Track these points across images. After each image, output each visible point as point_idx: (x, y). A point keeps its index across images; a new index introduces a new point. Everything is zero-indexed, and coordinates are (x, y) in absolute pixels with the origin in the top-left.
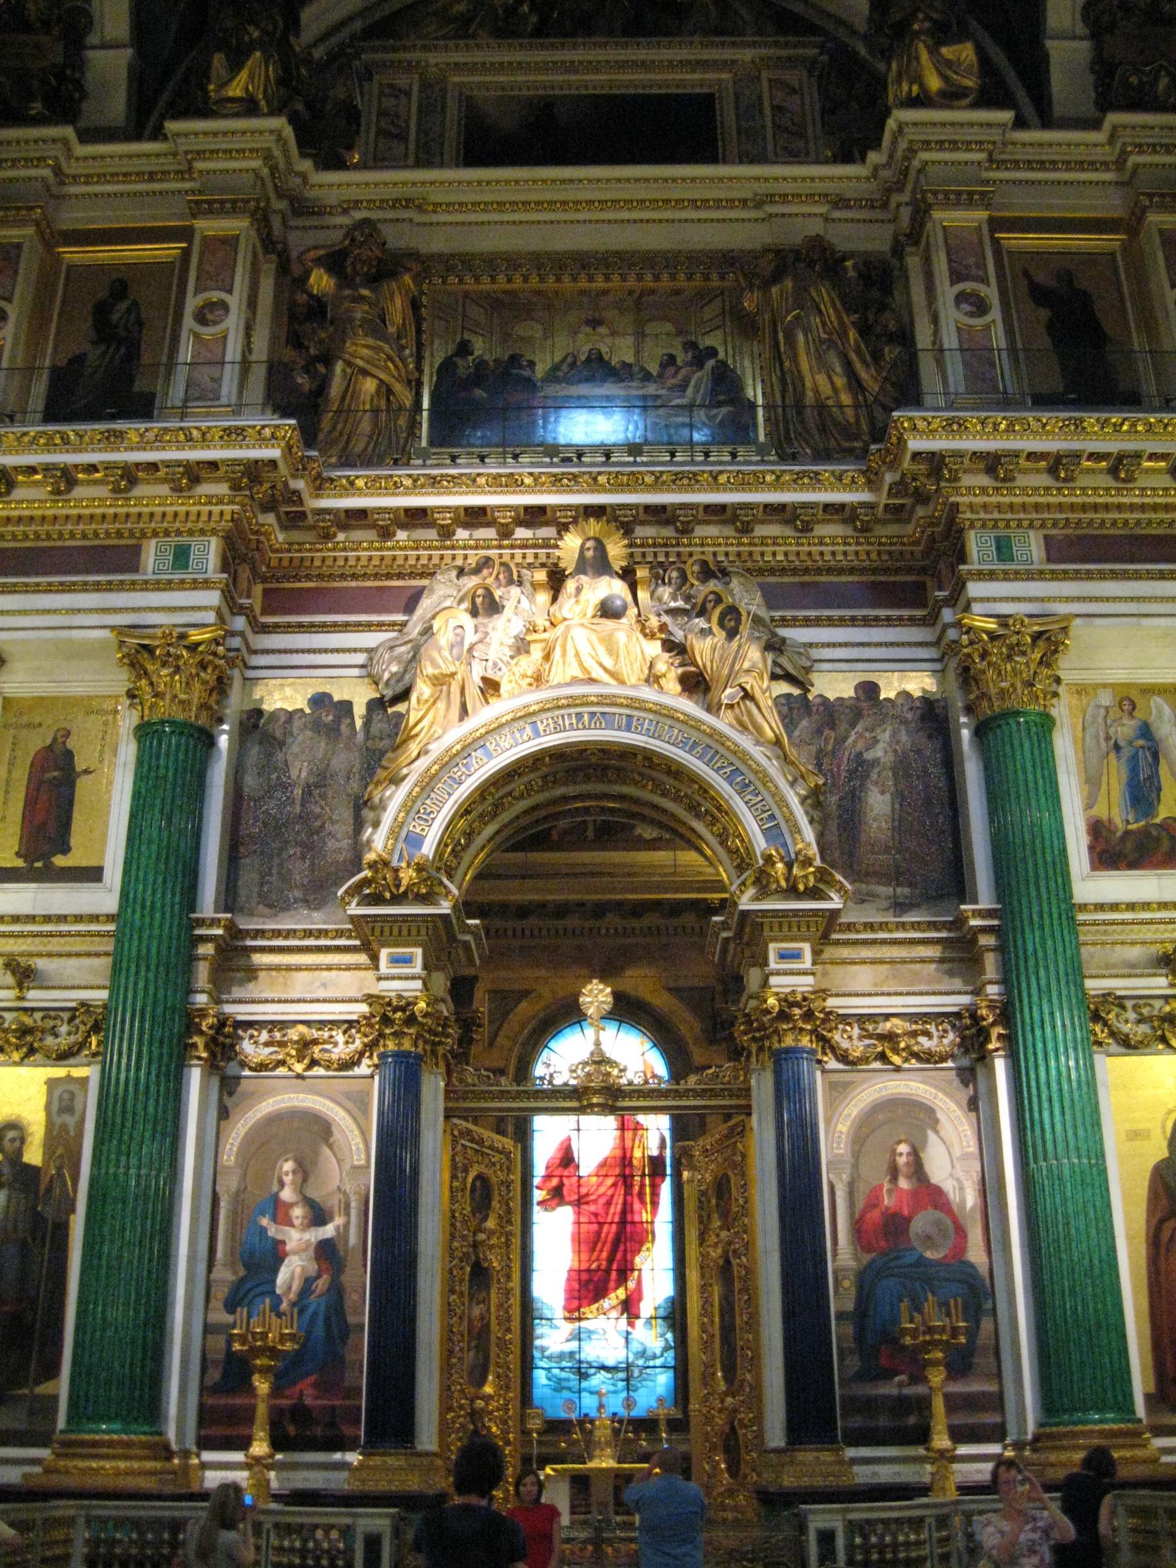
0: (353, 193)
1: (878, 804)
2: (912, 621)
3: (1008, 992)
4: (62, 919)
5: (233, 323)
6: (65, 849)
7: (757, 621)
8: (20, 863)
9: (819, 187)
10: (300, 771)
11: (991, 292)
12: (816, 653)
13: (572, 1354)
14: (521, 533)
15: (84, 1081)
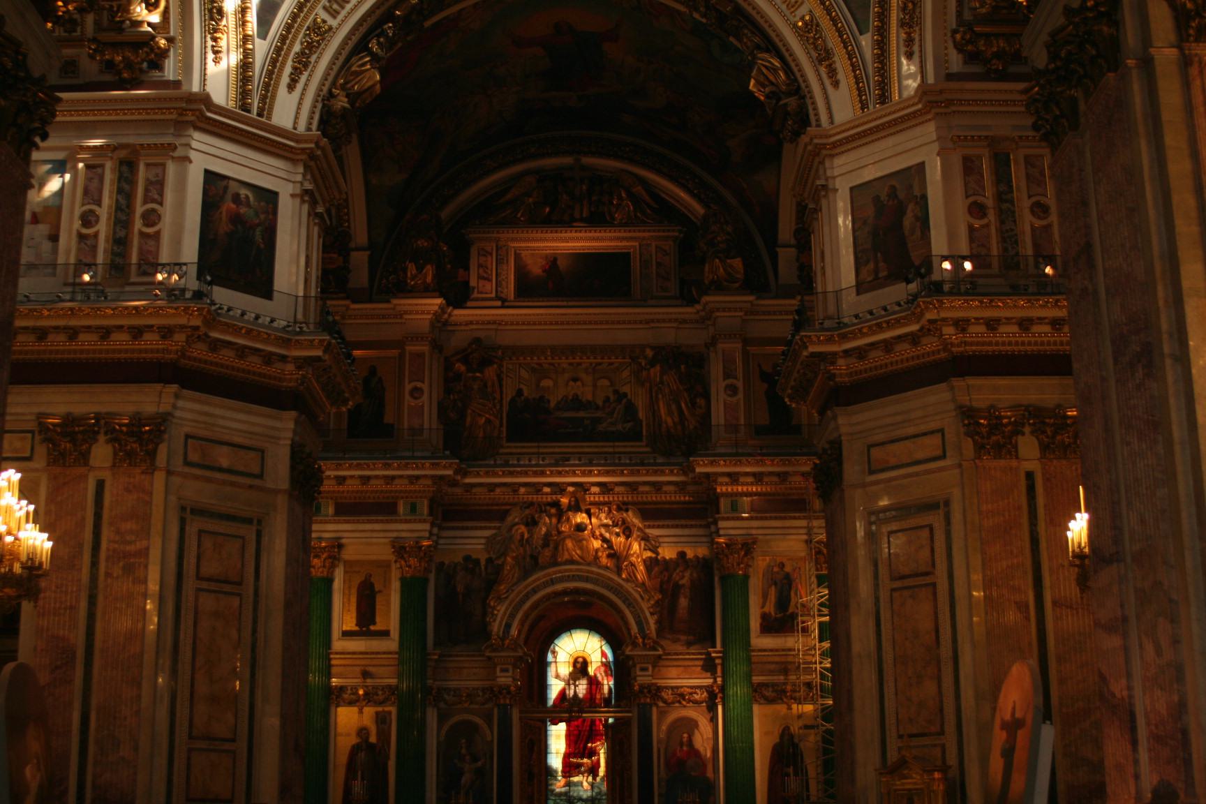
0: (471, 318)
1: (683, 602)
2: (701, 526)
3: (723, 681)
4: (378, 653)
5: (425, 397)
6: (374, 623)
7: (639, 529)
8: (357, 628)
9: (674, 316)
10: (460, 588)
11: (740, 384)
12: (661, 540)
13: (566, 794)
14: (547, 490)
15: (390, 713)
